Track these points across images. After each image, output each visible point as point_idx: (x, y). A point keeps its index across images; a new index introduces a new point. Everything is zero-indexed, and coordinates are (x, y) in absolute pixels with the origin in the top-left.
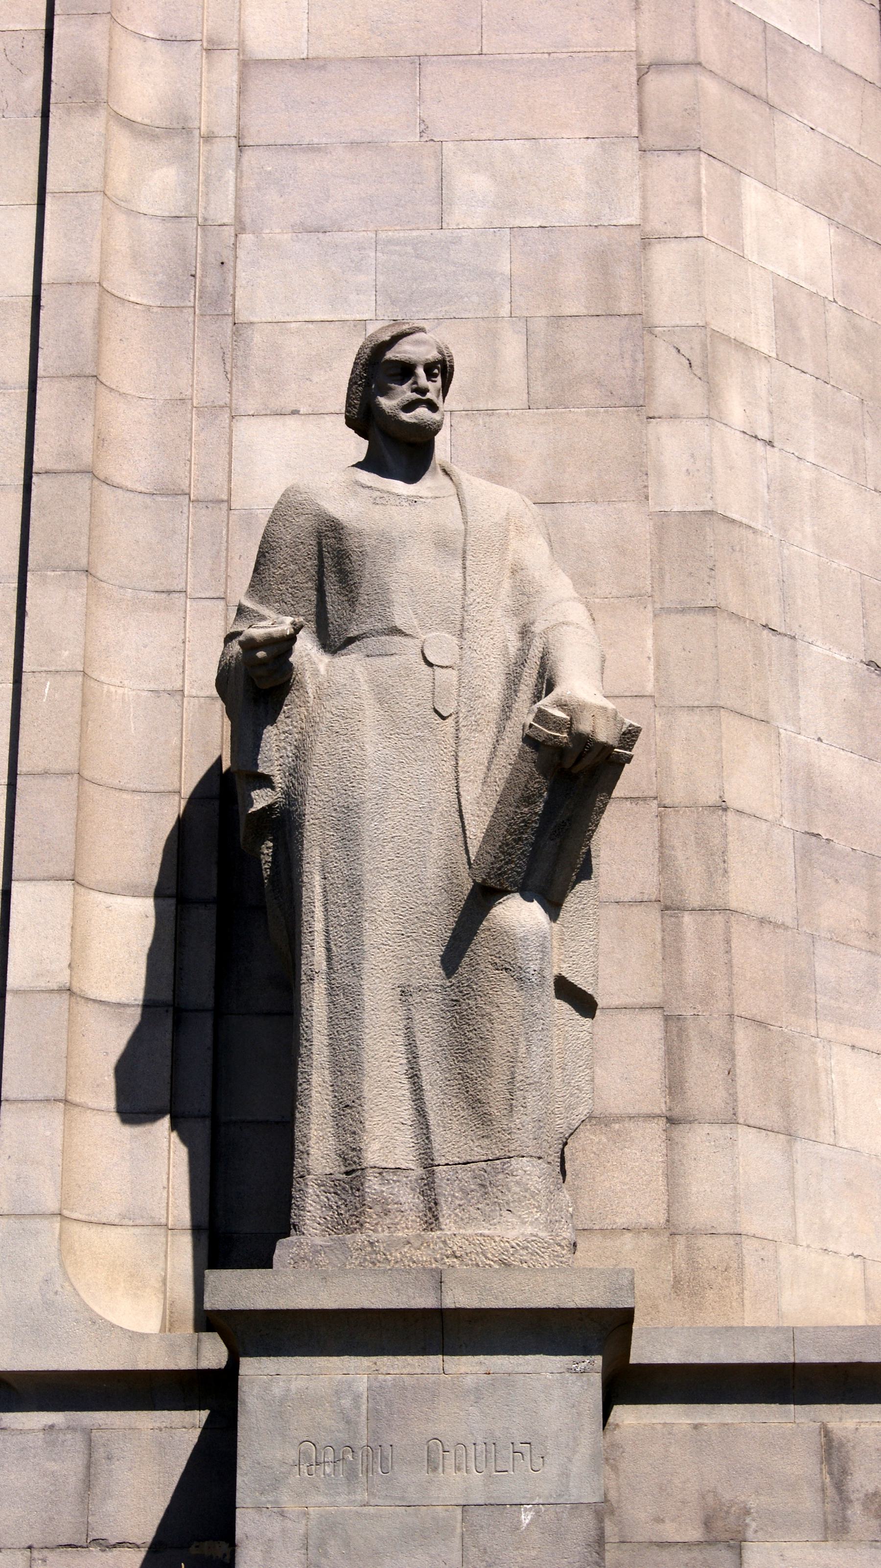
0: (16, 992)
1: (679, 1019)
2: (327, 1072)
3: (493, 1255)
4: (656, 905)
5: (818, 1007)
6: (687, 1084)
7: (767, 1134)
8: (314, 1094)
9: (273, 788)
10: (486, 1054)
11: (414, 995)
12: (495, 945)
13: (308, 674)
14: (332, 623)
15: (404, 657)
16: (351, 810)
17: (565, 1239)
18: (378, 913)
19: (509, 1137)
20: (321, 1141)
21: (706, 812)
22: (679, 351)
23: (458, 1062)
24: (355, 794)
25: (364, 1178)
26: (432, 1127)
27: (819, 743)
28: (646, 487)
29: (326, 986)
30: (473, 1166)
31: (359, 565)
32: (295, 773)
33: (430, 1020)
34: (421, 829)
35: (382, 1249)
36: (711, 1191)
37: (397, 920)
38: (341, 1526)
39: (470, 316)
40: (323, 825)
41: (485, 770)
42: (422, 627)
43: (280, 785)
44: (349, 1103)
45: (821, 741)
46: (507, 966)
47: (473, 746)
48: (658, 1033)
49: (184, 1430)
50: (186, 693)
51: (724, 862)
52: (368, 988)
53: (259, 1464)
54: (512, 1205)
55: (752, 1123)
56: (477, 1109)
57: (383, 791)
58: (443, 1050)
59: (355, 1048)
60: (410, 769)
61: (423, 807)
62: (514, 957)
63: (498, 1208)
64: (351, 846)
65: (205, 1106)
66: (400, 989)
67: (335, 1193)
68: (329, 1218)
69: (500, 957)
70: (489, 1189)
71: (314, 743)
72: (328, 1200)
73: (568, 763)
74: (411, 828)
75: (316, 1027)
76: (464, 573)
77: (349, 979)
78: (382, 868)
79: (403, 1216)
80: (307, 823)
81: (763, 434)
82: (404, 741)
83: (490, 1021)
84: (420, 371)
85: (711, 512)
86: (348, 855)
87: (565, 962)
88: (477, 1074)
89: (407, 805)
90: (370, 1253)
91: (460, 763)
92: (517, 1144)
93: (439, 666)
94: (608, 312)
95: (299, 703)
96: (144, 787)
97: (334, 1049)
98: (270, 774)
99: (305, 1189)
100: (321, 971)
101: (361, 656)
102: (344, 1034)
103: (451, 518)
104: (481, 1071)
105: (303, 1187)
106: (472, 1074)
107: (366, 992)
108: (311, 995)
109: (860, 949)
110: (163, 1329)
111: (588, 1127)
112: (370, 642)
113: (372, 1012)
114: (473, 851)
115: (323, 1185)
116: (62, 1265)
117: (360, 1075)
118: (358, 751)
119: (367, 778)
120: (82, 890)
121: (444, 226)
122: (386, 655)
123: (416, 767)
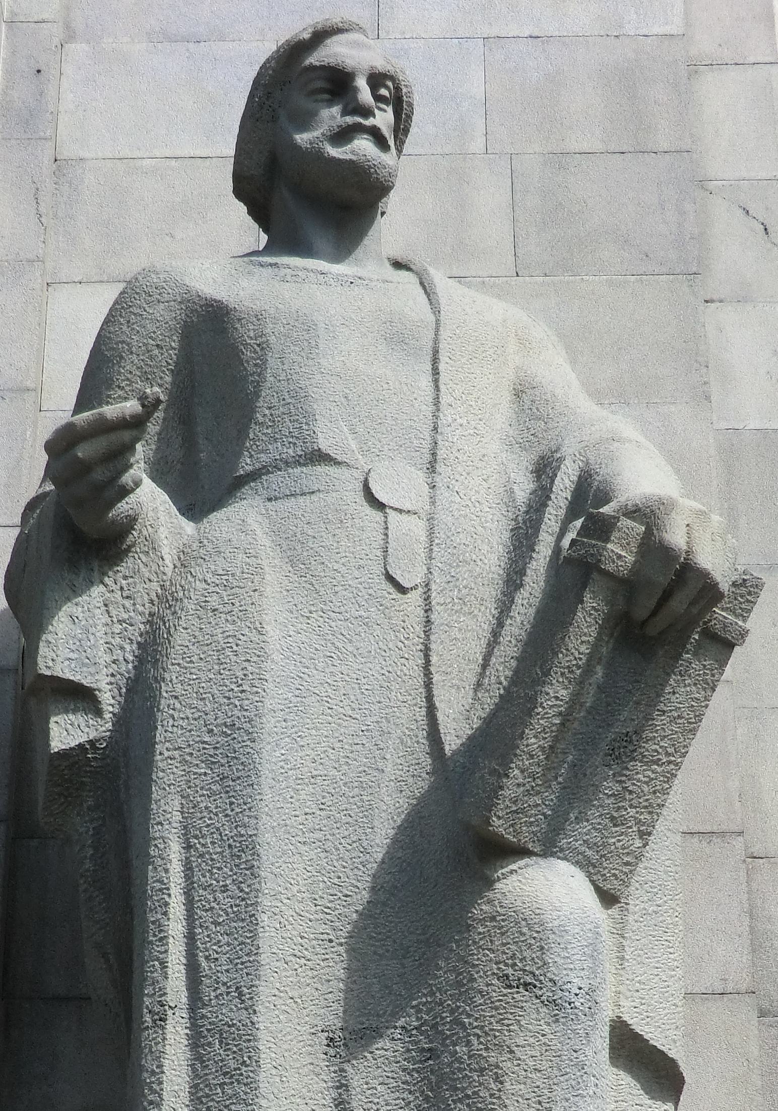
15: (334, 494)
16: (239, 729)
18: (285, 901)
24: (246, 702)
28: (705, 383)
29: (188, 1031)
31: (256, 365)
37: (322, 916)
39: (422, 151)
40: (188, 758)
46: (529, 979)
47: (455, 633)
57: (294, 700)
60: (344, 669)
61: (367, 730)
62: (541, 963)
66: (326, 1034)
71: (172, 630)
73: (642, 610)
76: (436, 382)
78: (293, 827)
80: (159, 757)
83: (498, 1079)
87: (627, 998)
89: (339, 725)
91: (434, 659)
93: (396, 509)
94: (638, 148)
95: (147, 575)
98: (94, 686)
101: (258, 501)
107: (263, 1035)
108: (160, 1047)
112: (275, 480)
113: (274, 1072)
123: (356, 666)
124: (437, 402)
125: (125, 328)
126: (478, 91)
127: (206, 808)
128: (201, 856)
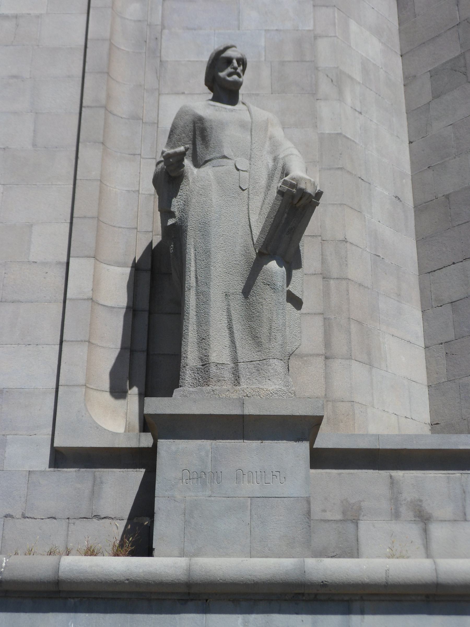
0: (71, 299)
1: (329, 319)
2: (195, 326)
3: (263, 396)
4: (321, 275)
5: (380, 319)
6: (332, 344)
7: (362, 365)
8: (189, 334)
9: (175, 217)
10: (260, 318)
11: (231, 296)
12: (264, 275)
13: (189, 174)
14: (199, 156)
15: (228, 166)
17: (292, 390)
19: (269, 351)
20: (193, 353)
21: (339, 243)
22: (328, 76)
23: (248, 322)
25: (210, 367)
26: (237, 347)
27: (379, 223)
30: (254, 363)
31: (210, 132)
32: (183, 211)
33: (237, 306)
34: (234, 232)
35: (218, 393)
36: (342, 385)
37: (224, 267)
38: (199, 505)
40: (195, 230)
41: (260, 210)
42: (235, 156)
43: (178, 216)
44: (204, 337)
45: (380, 222)
46: (269, 283)
48: (321, 323)
49: (133, 472)
50: (140, 192)
51: (346, 261)
52: (212, 292)
53: (165, 479)
54: (270, 377)
55: (357, 360)
56: (256, 340)
57: (219, 217)
58: (242, 317)
59: (207, 316)
60: (229, 209)
62: (272, 280)
63: (264, 379)
64: (206, 237)
65: (145, 347)
67: (198, 373)
68: (195, 383)
69: (266, 280)
70: (261, 371)
72: (195, 376)
74: (230, 232)
75: (191, 308)
77: (205, 289)
79: (225, 383)
81: (358, 109)
82: (227, 198)
84: (235, 61)
85: (340, 134)
86: (205, 241)
88: (256, 326)
89: (229, 223)
90: (212, 395)
91: (250, 207)
92: (272, 354)
93: (241, 170)
95: (186, 184)
96: (123, 226)
97: (198, 316)
98: (174, 211)
99: (185, 372)
100: (193, 286)
102: (202, 310)
103: (246, 117)
104: (258, 325)
105: (184, 371)
106: (254, 326)
109: (394, 300)
110: (125, 431)
111: (294, 358)
112: (214, 162)
113: (214, 302)
114: (255, 240)
115: (193, 370)
116: (85, 405)
117: (209, 326)
118: (209, 201)
119: (213, 211)
120: (98, 262)
121: (240, 28)
122: (221, 166)
124: (251, 142)
125: (180, 121)
126: (263, 44)
127: (199, 242)
128: (198, 253)
